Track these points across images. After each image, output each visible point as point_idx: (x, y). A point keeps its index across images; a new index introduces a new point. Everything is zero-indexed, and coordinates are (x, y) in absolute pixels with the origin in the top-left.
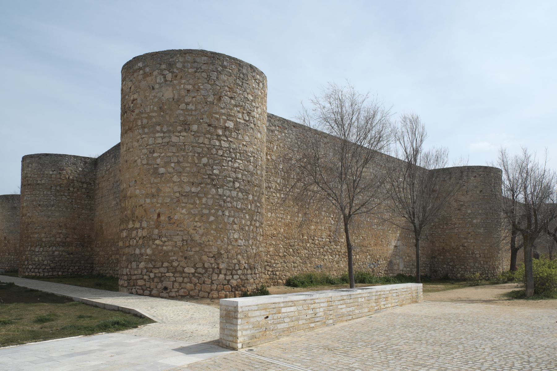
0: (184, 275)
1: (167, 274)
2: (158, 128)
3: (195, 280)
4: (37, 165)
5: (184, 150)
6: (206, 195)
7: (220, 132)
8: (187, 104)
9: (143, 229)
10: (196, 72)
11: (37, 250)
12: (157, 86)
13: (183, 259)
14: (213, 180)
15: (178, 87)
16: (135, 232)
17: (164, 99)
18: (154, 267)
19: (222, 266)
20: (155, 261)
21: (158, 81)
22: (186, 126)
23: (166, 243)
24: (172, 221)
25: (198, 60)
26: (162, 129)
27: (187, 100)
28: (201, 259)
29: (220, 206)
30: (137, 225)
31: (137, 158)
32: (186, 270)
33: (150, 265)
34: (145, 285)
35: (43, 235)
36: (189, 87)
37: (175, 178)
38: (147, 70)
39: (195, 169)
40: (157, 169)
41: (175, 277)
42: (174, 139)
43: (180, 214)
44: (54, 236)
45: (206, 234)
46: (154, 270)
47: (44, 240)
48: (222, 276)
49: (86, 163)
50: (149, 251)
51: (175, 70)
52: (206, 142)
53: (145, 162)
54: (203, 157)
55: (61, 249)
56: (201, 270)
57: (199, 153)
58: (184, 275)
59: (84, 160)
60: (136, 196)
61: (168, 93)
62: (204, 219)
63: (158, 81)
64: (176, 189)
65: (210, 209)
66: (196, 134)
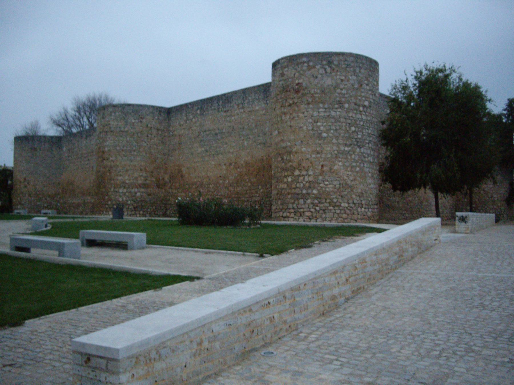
0: (341, 208)
1: (330, 208)
2: (321, 105)
3: (348, 211)
4: (120, 113)
5: (340, 122)
6: (354, 152)
7: (361, 109)
8: (341, 89)
9: (309, 175)
10: (347, 67)
11: (121, 191)
12: (319, 76)
13: (340, 197)
14: (358, 142)
15: (335, 77)
16: (302, 178)
17: (325, 86)
18: (319, 203)
19: (364, 202)
20: (320, 198)
21: (320, 72)
22: (340, 104)
23: (329, 186)
24: (332, 171)
25: (348, 59)
26: (324, 106)
27: (342, 86)
28: (351, 197)
29: (362, 160)
30: (304, 173)
31: (302, 125)
32: (343, 205)
33: (316, 201)
34: (312, 215)
35: (127, 177)
36: (343, 78)
37: (334, 141)
38: (311, 64)
39: (347, 135)
40: (320, 134)
41: (335, 210)
42: (333, 113)
43: (338, 166)
44: (136, 179)
45: (355, 180)
46: (319, 205)
47: (127, 182)
48: (363, 209)
49: (160, 112)
50: (315, 192)
51: (333, 66)
52: (354, 116)
53: (310, 128)
54: (352, 126)
55: (142, 190)
56: (352, 205)
57: (349, 124)
58: (341, 208)
59: (160, 110)
60: (302, 152)
61: (328, 82)
62: (353, 169)
63: (320, 72)
64: (335, 148)
65: (356, 163)
66: (347, 112)
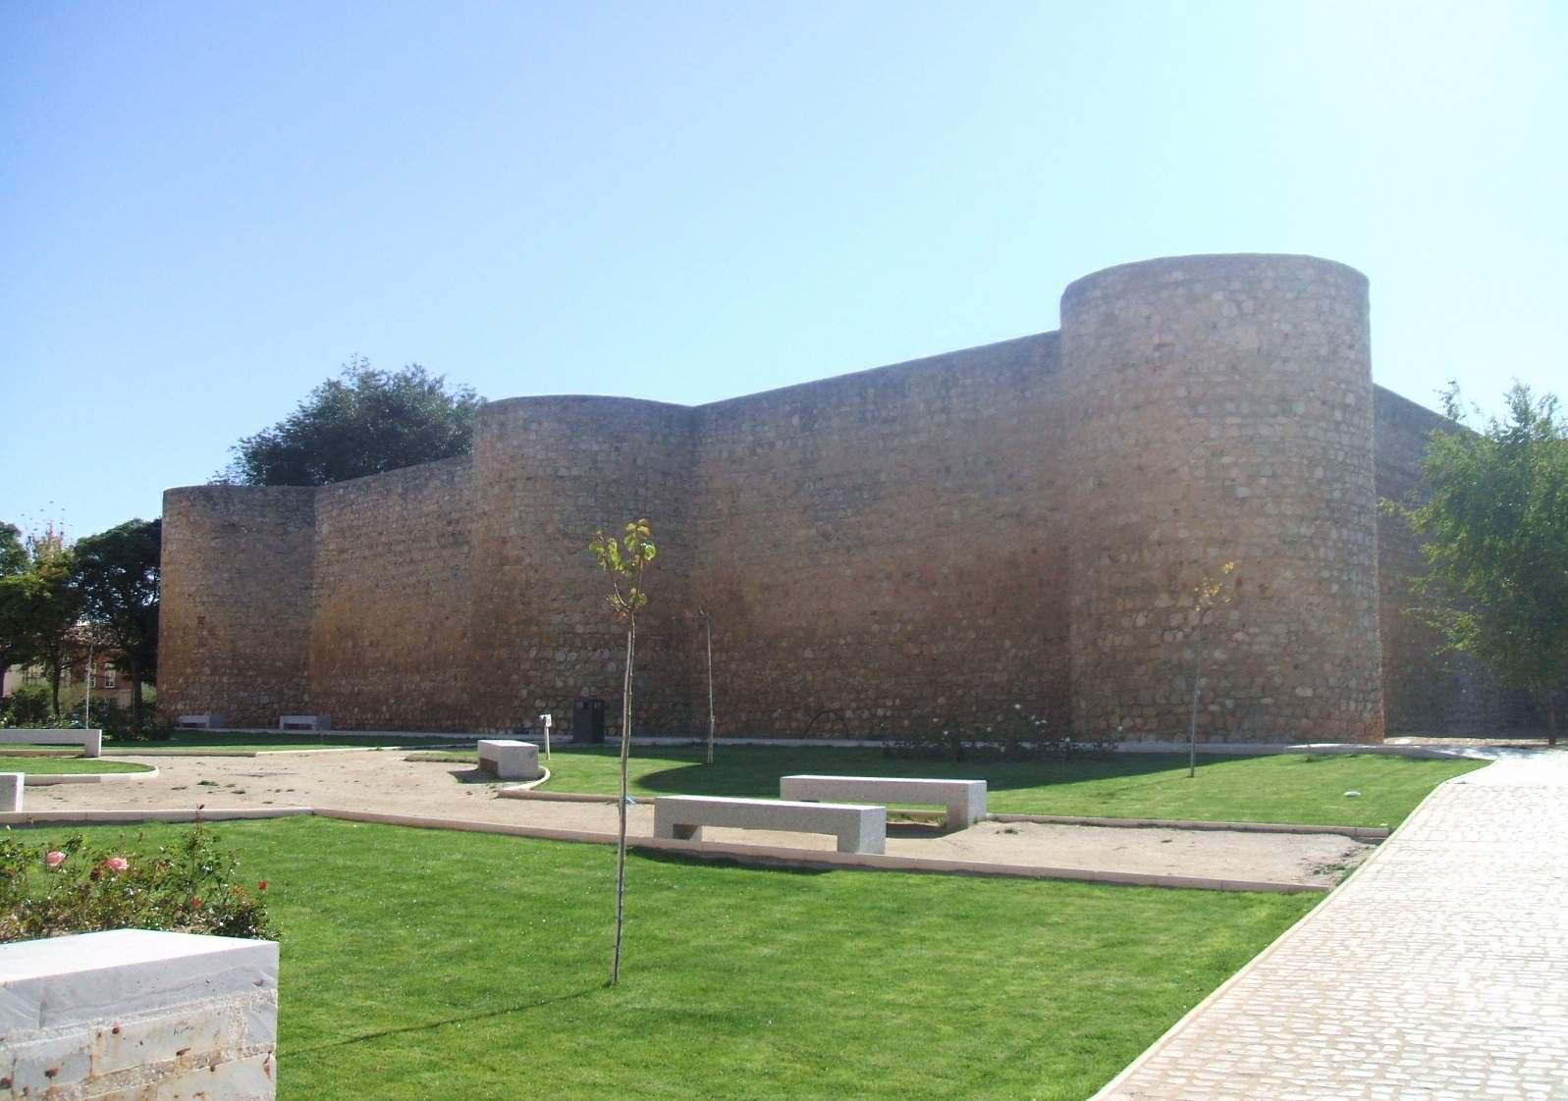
7: (1338, 416)
8: (1285, 361)
24: (1268, 593)
36: (1287, 328)
37: (1270, 508)
42: (1265, 431)
47: (580, 629)
